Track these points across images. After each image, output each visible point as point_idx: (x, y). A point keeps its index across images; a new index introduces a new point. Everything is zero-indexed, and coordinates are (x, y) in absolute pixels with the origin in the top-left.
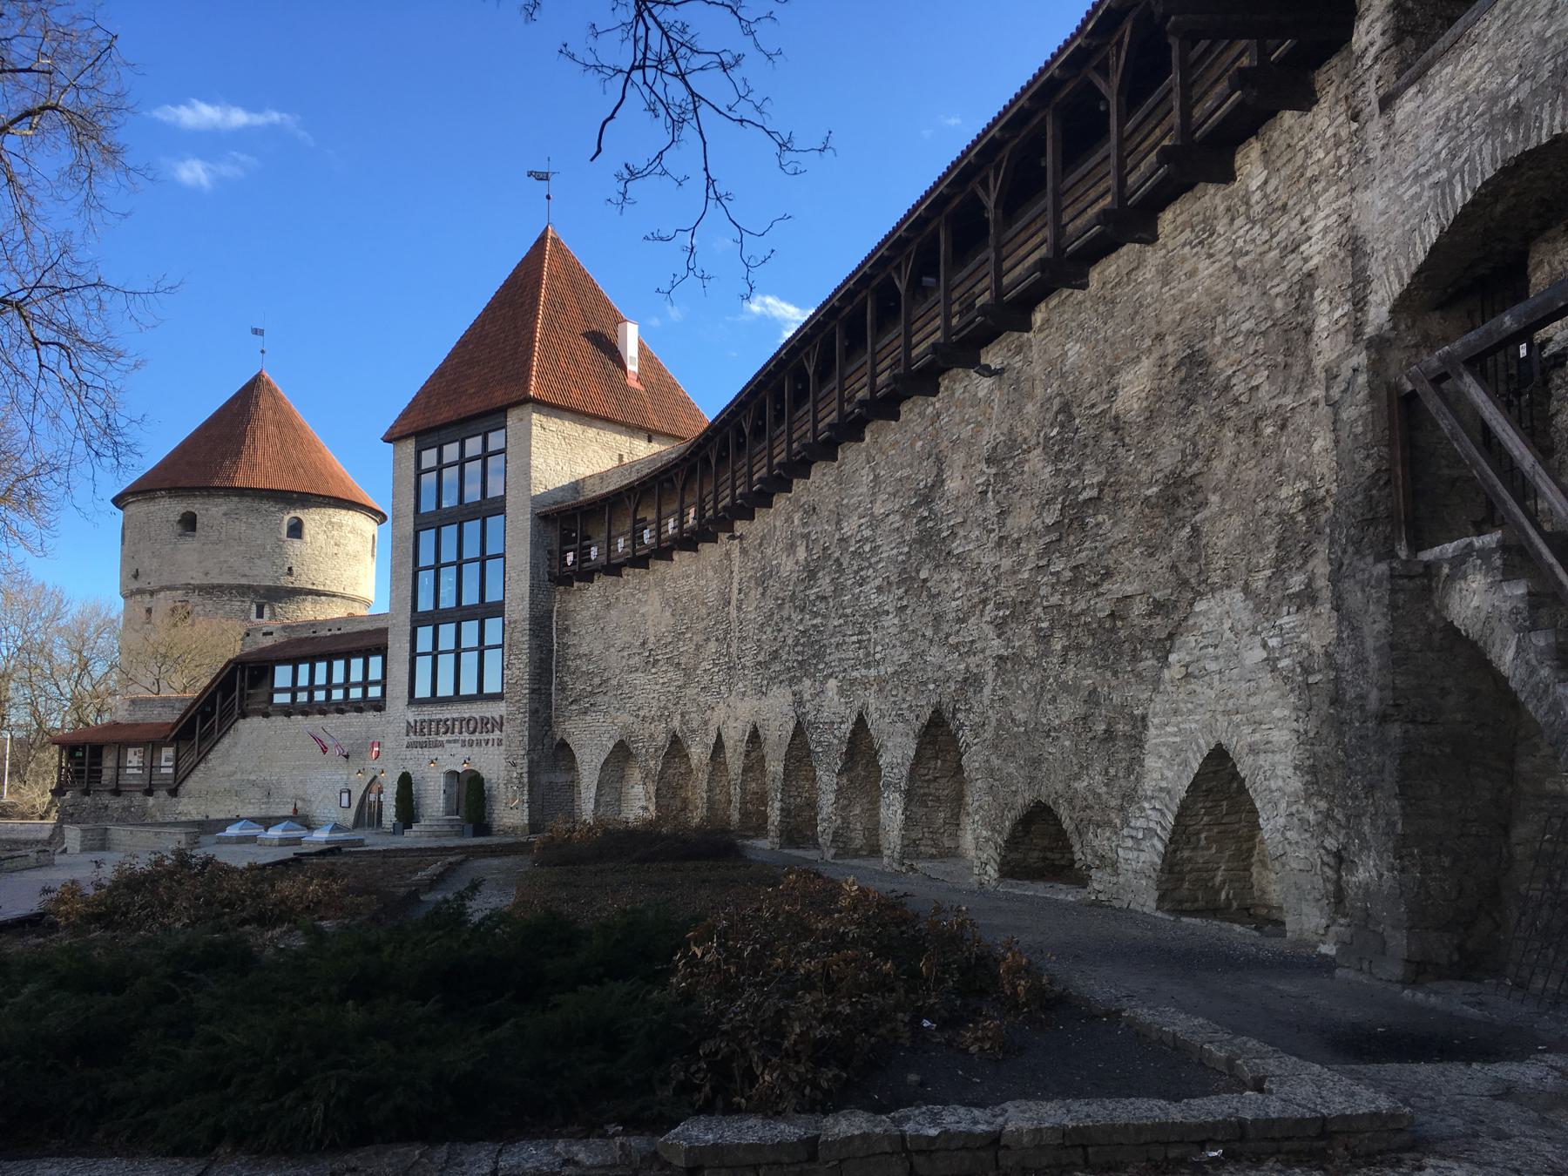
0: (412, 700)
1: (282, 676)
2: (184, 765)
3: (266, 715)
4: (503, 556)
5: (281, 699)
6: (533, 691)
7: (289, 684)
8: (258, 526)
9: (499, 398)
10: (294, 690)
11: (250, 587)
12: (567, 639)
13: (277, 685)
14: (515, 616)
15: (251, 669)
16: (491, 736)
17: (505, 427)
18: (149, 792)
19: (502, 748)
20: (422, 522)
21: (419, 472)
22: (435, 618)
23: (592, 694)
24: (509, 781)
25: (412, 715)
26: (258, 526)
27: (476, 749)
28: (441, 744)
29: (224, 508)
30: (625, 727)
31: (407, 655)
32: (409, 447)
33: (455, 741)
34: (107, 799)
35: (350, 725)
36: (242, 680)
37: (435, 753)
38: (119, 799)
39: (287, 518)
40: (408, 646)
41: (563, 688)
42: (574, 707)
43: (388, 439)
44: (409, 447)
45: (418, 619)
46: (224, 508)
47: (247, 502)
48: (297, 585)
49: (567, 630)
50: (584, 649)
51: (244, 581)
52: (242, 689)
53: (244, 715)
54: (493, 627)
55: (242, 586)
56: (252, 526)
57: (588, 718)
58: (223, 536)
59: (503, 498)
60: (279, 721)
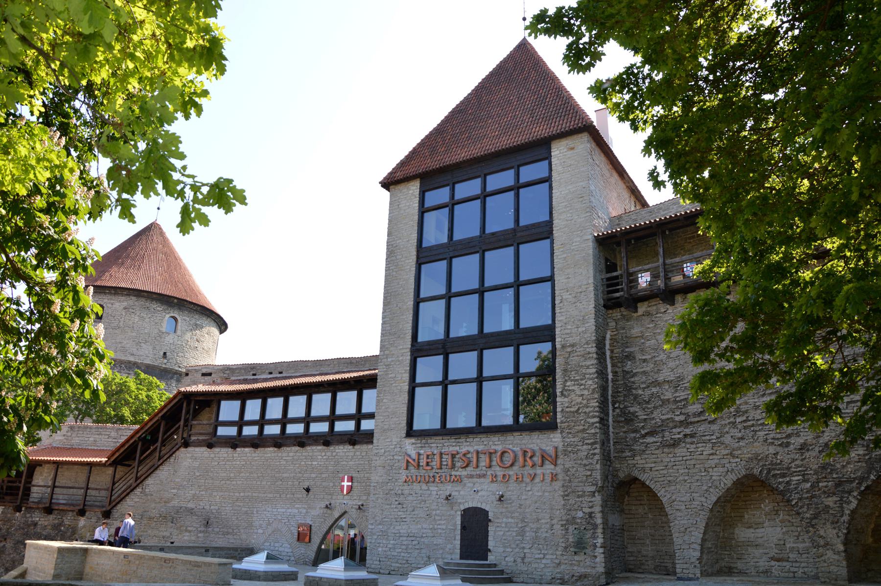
0: (410, 432)
1: (229, 410)
2: (120, 487)
3: (210, 446)
4: (551, 279)
5: (222, 431)
6: (602, 419)
7: (236, 418)
8: (147, 320)
9: (540, 131)
10: (241, 423)
11: (135, 363)
12: (629, 366)
13: (222, 418)
14: (571, 340)
15: (197, 402)
16: (539, 471)
17: (548, 157)
18: (82, 513)
19: (558, 485)
20: (425, 255)
21: (423, 211)
22: (446, 347)
23: (685, 423)
24: (572, 521)
25: (411, 447)
26: (147, 320)
27: (512, 485)
28: (459, 480)
29: (125, 304)
30: (756, 457)
31: (406, 387)
32: (414, 187)
33: (480, 476)
34: (38, 517)
35: (312, 459)
36: (188, 412)
37: (448, 488)
38: (51, 517)
39: (168, 316)
40: (406, 377)
41: (628, 419)
42: (650, 440)
43: (387, 184)
44: (414, 187)
45: (419, 350)
46: (125, 304)
47: (142, 302)
48: (168, 366)
49: (630, 357)
50: (666, 374)
51: (132, 359)
52: (186, 420)
53: (186, 444)
54: (369, 395)
55: (130, 362)
56: (142, 318)
57: (680, 451)
58: (121, 324)
59: (549, 224)
60: (223, 453)
